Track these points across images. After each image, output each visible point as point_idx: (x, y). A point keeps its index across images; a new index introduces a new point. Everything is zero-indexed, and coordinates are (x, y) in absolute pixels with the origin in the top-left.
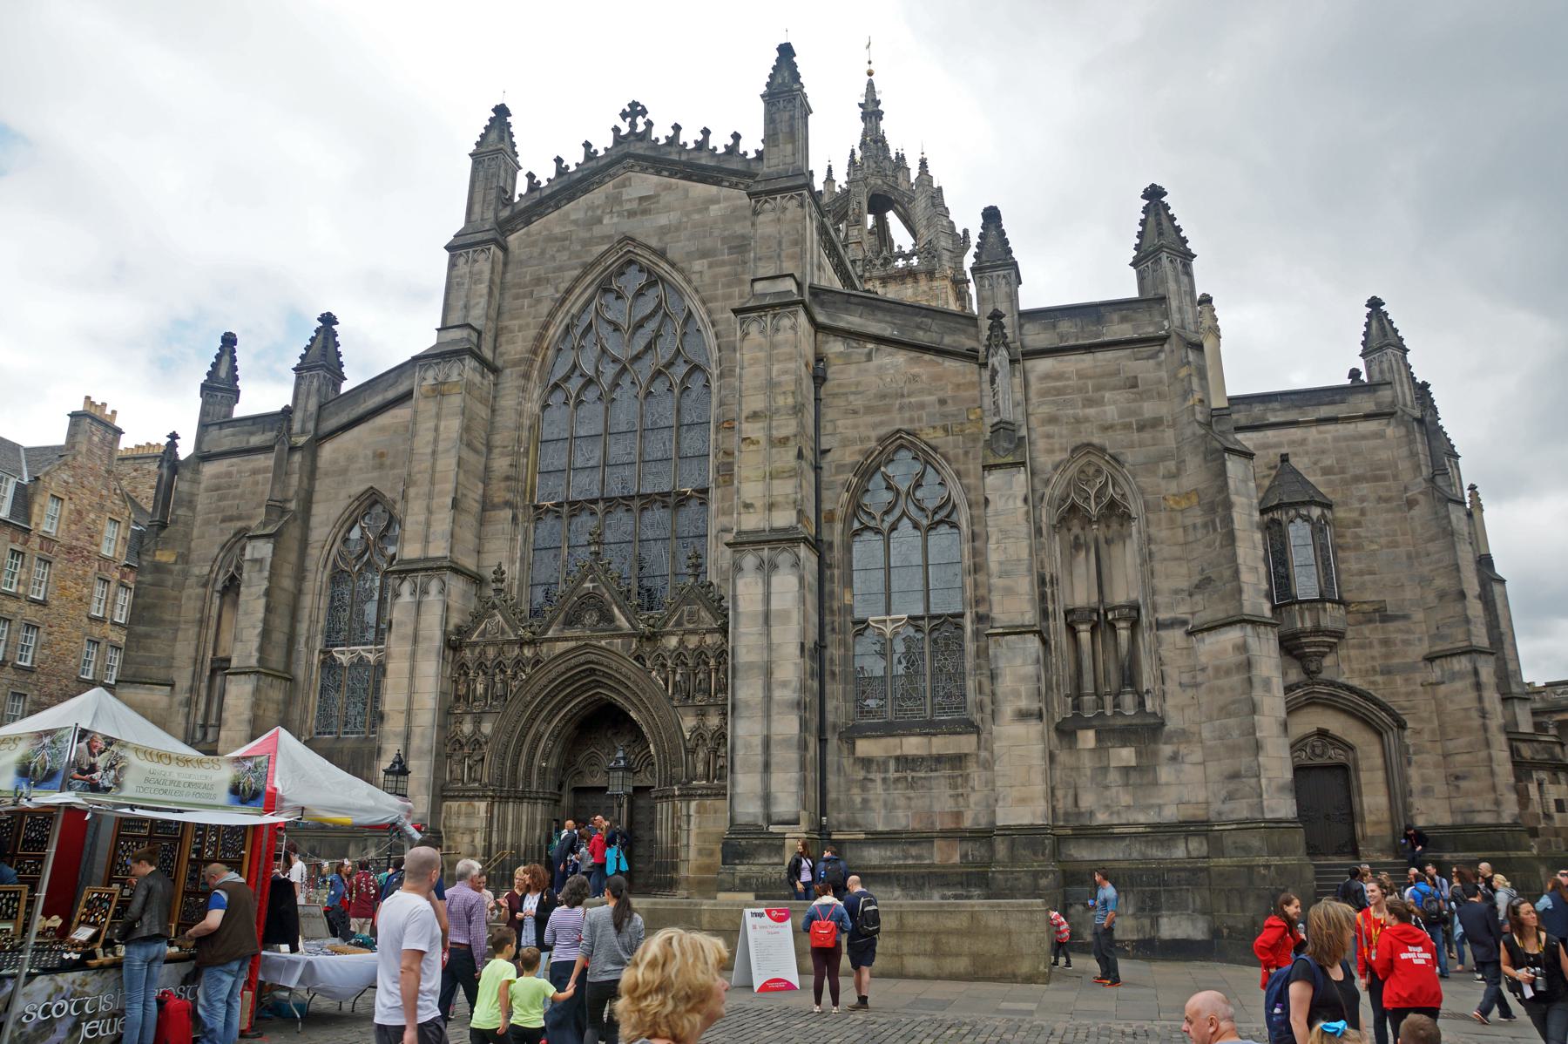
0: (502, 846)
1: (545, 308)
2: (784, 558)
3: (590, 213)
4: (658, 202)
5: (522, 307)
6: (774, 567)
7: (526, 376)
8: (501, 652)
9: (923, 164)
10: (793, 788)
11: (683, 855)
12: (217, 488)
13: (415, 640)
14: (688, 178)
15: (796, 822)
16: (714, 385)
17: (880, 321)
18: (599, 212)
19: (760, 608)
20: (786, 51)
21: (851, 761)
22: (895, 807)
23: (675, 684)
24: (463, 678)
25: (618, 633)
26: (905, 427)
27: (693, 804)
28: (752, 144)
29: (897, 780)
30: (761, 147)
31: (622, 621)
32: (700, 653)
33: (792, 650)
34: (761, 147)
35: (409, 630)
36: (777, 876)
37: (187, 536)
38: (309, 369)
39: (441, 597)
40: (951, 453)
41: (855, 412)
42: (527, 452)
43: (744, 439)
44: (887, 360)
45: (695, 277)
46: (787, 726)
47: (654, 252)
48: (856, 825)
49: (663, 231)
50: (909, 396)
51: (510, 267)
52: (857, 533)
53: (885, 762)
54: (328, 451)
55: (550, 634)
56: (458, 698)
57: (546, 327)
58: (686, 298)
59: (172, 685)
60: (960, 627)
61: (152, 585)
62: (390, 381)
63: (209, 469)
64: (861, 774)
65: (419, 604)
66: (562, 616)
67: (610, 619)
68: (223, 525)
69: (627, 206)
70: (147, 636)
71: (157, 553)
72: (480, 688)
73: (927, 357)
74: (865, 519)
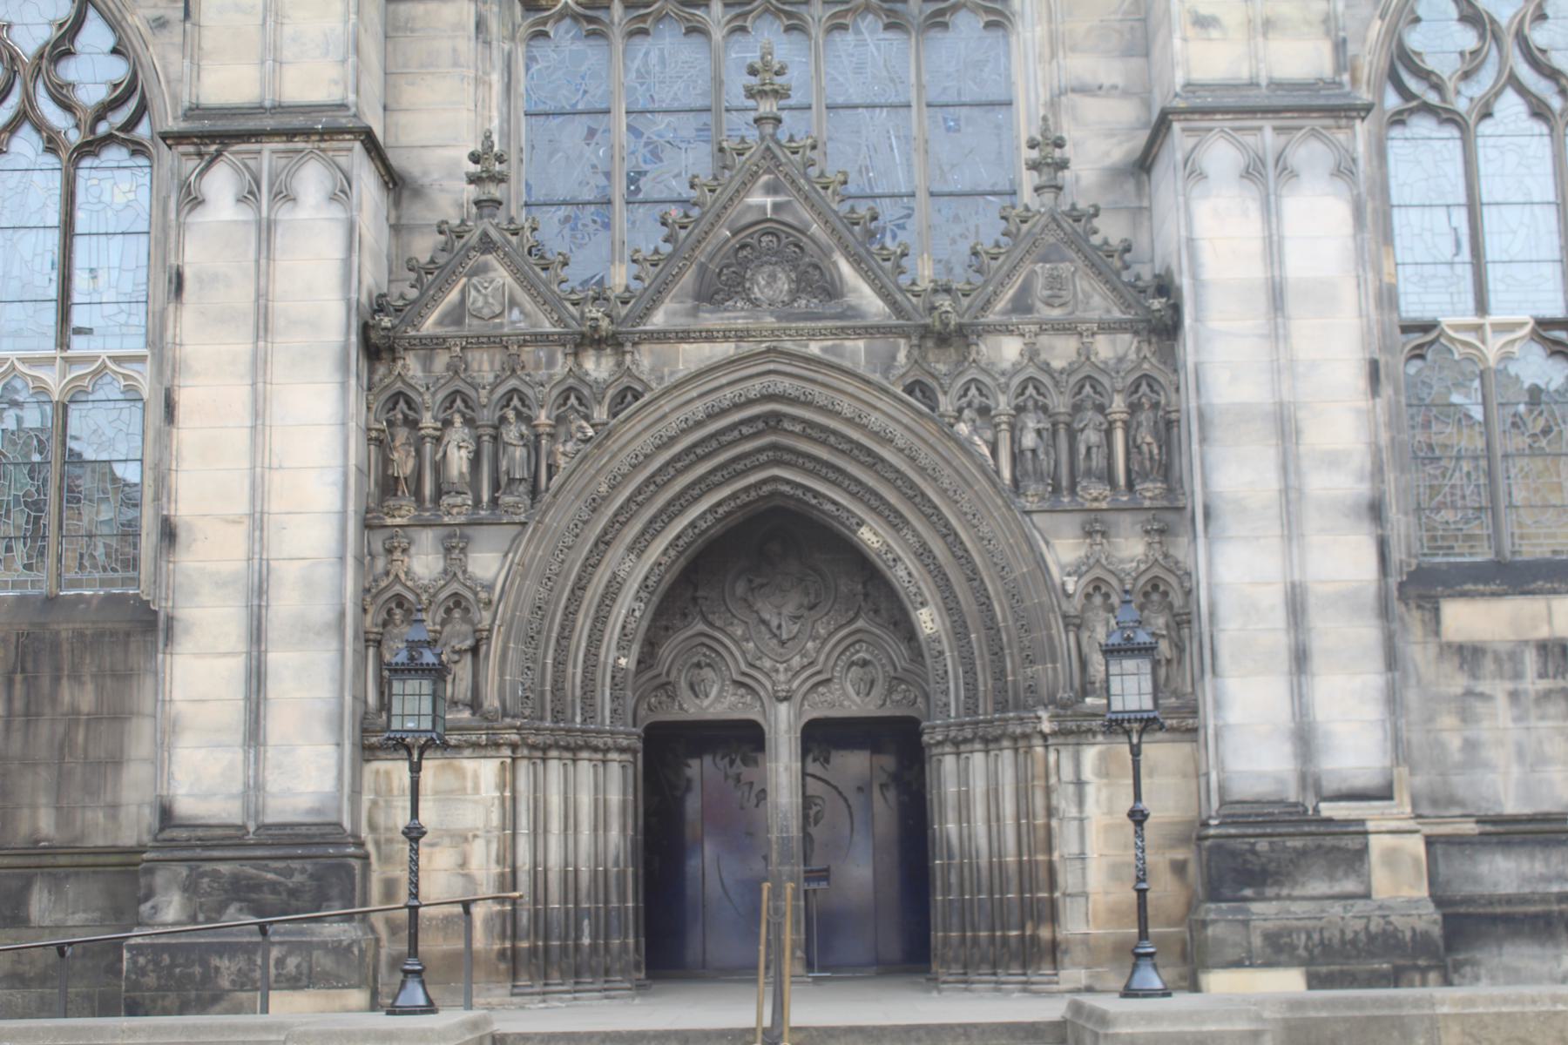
0: (539, 875)
2: (1310, 154)
6: (1286, 171)
10: (1373, 711)
11: (1068, 879)
13: (263, 323)
15: (1385, 794)
19: (1256, 271)
21: (1432, 650)
22: (1542, 760)
23: (1016, 457)
24: (402, 434)
25: (854, 325)
27: (1090, 755)
29: (1546, 695)
33: (1348, 375)
35: (242, 296)
36: (1359, 925)
39: (337, 212)
48: (1452, 801)
52: (1398, 119)
53: (1514, 656)
55: (658, 320)
56: (389, 486)
64: (1458, 683)
65: (266, 231)
66: (689, 277)
67: (831, 290)
72: (458, 461)
74: (1413, 84)
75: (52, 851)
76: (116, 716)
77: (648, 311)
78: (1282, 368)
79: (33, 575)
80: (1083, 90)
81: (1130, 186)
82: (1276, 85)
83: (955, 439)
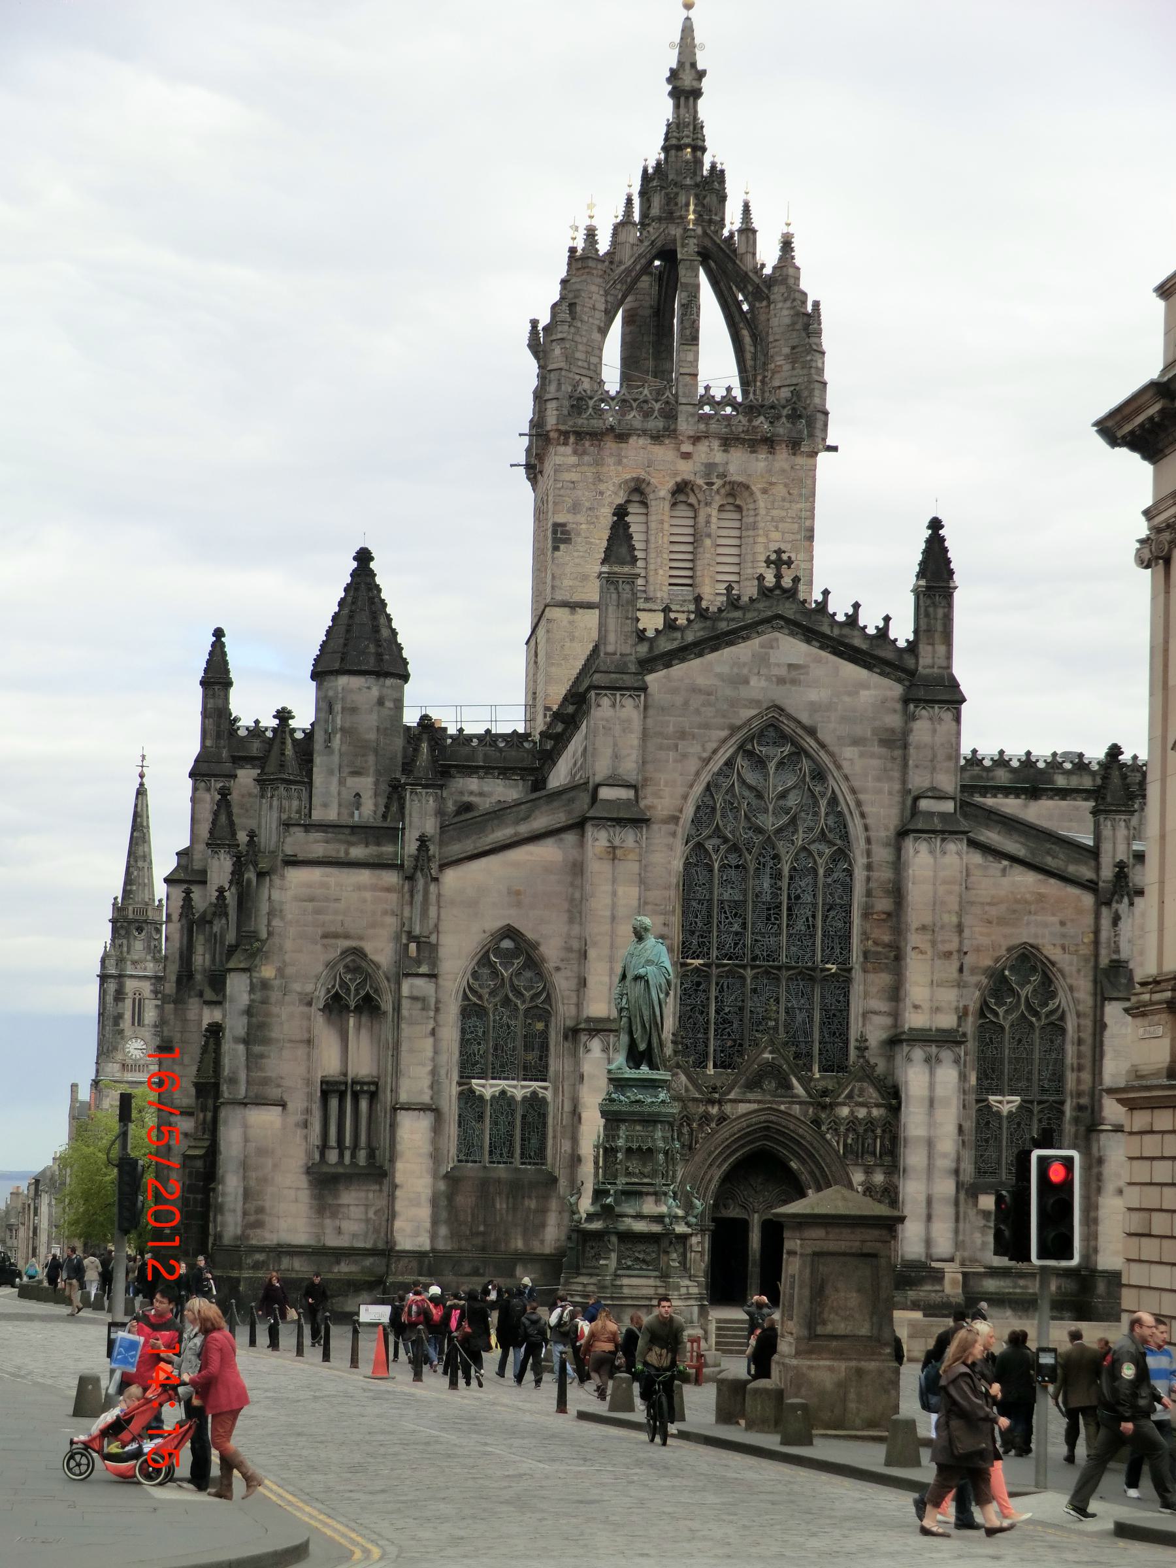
1: (693, 765)
2: (947, 1055)
3: (736, 670)
4: (807, 674)
5: (667, 761)
6: (939, 1061)
7: (674, 834)
8: (685, 1107)
9: (787, 245)
10: (950, 1235)
12: (311, 899)
14: (840, 655)
15: (952, 1260)
16: (859, 874)
17: (1017, 842)
18: (745, 671)
19: (926, 1093)
20: (936, 525)
23: (845, 1145)
26: (1031, 941)
28: (902, 632)
30: (911, 638)
31: (799, 1089)
32: (870, 1123)
34: (911, 638)
37: (281, 948)
38: (425, 786)
40: (1067, 969)
41: (990, 922)
42: (674, 911)
43: (914, 948)
44: (1018, 879)
45: (846, 765)
46: (946, 1187)
47: (804, 727)
48: (976, 1261)
49: (814, 707)
50: (1035, 914)
51: (651, 712)
54: (452, 878)
55: (732, 1096)
57: (691, 786)
58: (830, 778)
59: (284, 1105)
60: (1062, 1113)
61: (263, 1002)
62: (522, 815)
63: (297, 877)
67: (789, 1087)
68: (326, 941)
69: (775, 671)
70: (262, 1056)
71: (263, 968)
73: (1052, 881)
75: (523, 1254)
76: (543, 1211)
77: (729, 1093)
78: (931, 1124)
79: (509, 1160)
80: (875, 1013)
81: (888, 1048)
82: (940, 1031)
83: (825, 1139)
